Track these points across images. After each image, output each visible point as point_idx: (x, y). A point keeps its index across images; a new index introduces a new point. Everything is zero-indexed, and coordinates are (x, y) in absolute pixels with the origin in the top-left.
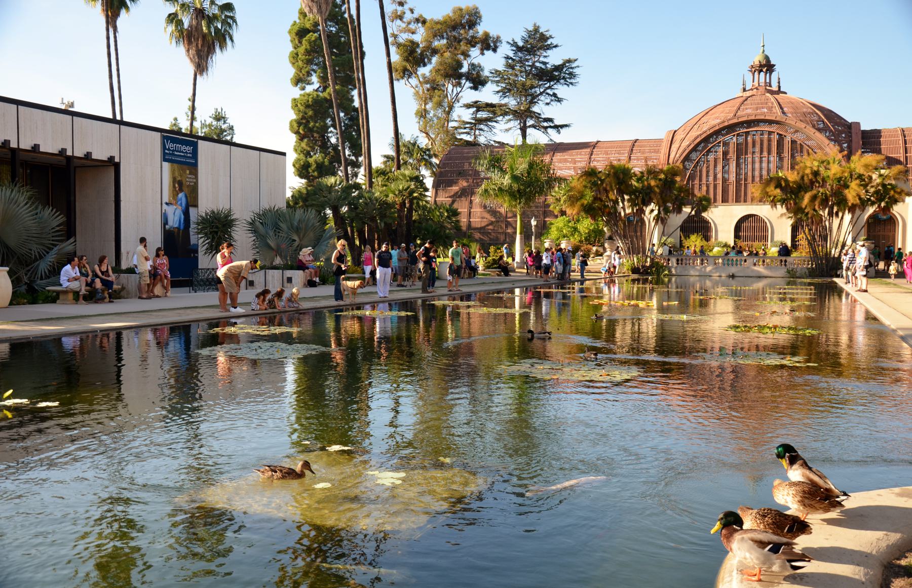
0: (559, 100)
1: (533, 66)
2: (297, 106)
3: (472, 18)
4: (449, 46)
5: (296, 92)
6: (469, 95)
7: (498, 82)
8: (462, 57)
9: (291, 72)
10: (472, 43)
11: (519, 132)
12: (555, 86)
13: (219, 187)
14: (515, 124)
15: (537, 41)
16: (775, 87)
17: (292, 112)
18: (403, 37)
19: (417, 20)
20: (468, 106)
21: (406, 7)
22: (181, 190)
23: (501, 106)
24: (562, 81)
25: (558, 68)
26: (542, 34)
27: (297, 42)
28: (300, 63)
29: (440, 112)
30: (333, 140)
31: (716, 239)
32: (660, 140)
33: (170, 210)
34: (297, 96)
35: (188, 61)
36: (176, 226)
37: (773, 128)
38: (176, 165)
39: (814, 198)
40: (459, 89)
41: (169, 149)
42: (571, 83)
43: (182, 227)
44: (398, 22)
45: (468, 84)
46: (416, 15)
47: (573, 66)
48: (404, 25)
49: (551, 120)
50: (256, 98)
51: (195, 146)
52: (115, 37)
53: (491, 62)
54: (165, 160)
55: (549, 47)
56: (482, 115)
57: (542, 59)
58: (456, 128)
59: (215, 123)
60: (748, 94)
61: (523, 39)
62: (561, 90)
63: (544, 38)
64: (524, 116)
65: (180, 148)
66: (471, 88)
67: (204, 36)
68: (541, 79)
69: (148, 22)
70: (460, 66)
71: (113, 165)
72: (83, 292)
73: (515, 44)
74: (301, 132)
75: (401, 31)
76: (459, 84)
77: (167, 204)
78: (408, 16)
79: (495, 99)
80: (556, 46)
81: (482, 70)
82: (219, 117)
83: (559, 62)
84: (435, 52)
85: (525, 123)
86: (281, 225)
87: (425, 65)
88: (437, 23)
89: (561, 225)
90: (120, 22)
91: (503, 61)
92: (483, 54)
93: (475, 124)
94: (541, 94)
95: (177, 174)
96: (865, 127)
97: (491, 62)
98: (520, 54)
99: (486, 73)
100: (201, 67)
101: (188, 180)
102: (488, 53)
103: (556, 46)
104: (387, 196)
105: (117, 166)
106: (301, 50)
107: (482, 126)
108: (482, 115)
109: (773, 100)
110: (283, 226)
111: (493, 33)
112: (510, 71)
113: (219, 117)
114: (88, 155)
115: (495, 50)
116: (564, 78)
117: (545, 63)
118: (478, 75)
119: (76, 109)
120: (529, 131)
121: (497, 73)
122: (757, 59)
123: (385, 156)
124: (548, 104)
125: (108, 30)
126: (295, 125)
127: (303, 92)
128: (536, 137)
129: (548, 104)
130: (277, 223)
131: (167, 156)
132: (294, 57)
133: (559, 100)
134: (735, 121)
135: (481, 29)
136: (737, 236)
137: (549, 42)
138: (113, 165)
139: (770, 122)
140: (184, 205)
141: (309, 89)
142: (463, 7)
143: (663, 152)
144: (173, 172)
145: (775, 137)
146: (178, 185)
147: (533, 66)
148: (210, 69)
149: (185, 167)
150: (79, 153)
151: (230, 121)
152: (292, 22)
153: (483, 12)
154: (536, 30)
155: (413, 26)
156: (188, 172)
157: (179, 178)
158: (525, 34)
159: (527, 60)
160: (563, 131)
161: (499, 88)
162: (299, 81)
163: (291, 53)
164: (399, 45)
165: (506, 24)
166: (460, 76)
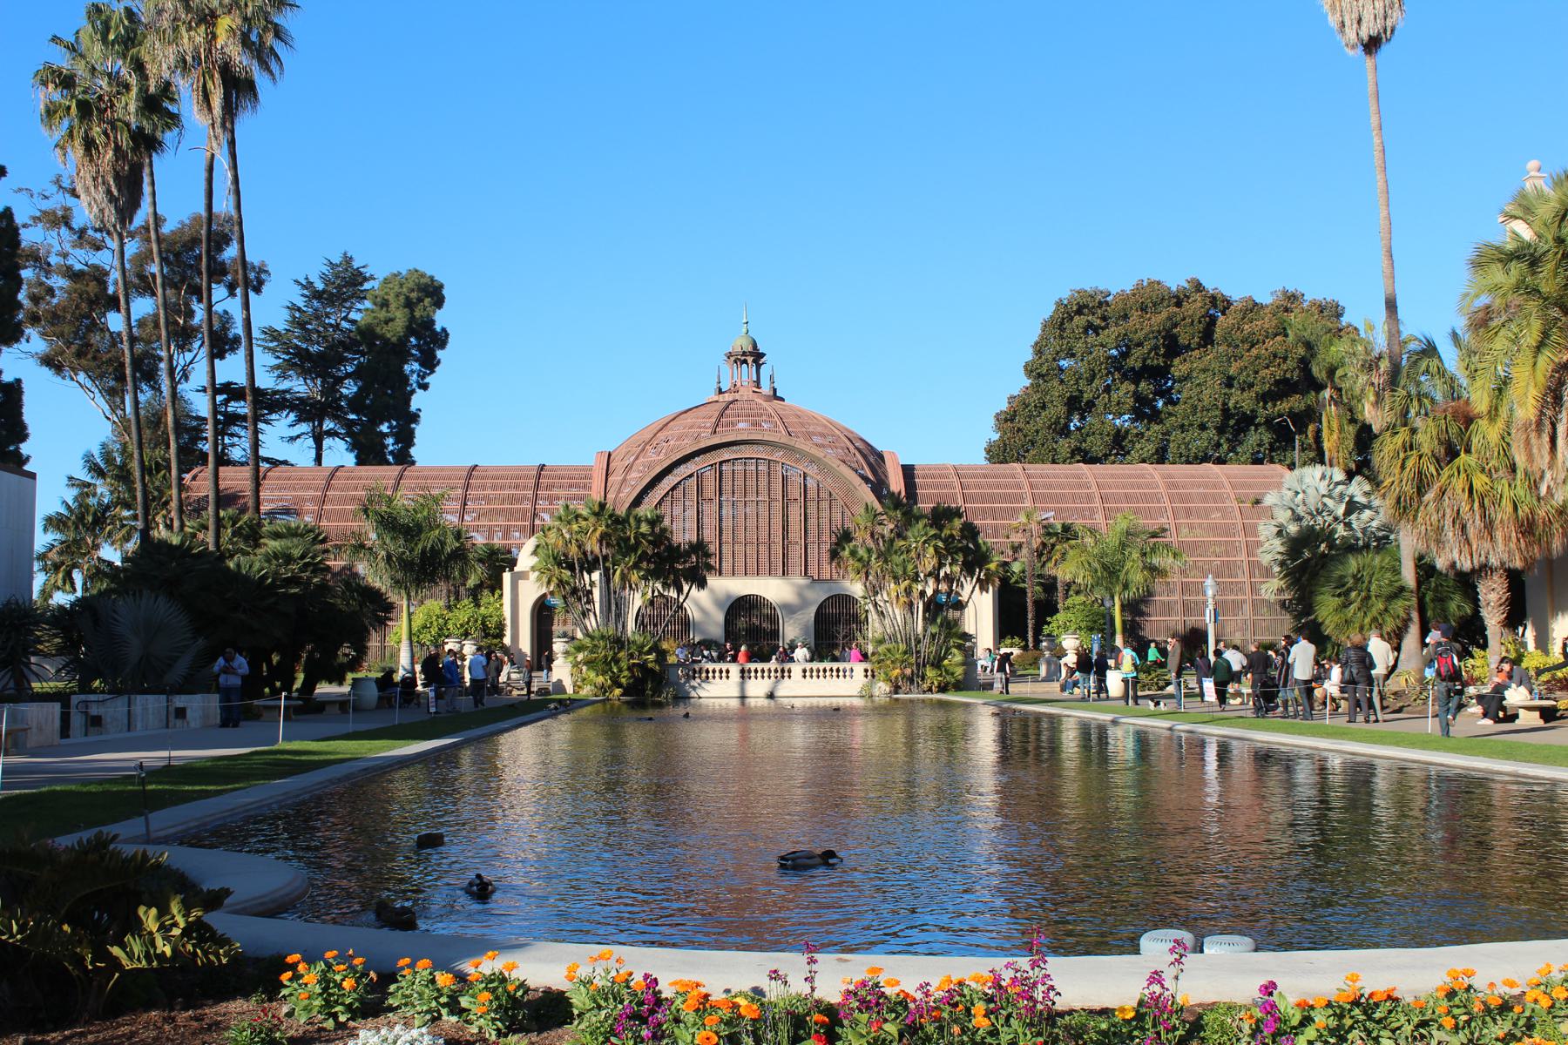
11: (311, 442)
61: (323, 277)
73: (309, 285)
91: (286, 315)
120: (327, 442)
154: (348, 260)
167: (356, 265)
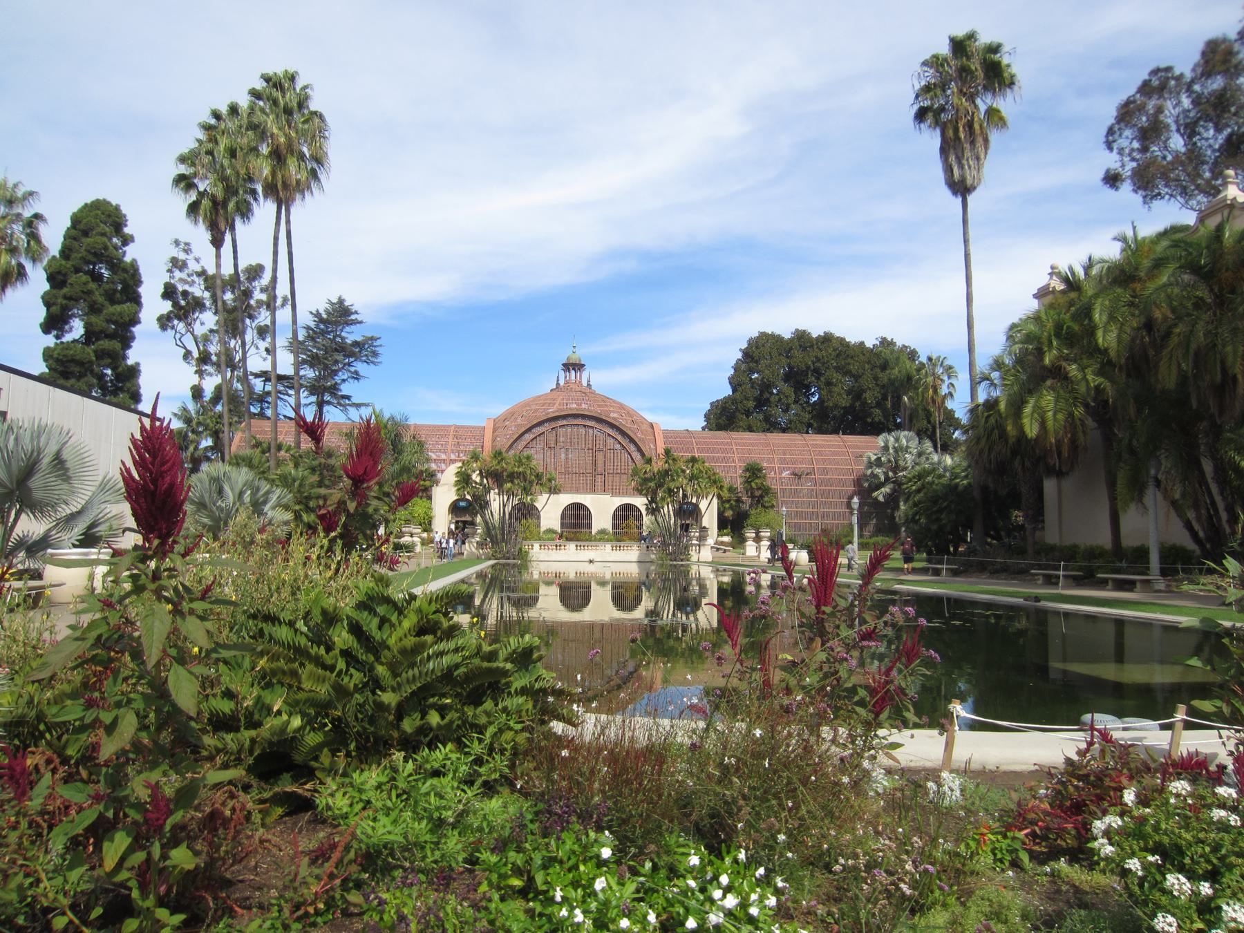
5: (50, 341)
15: (341, 314)
17: (44, 364)
25: (356, 344)
49: (348, 398)
57: (343, 334)
62: (360, 367)
73: (318, 315)
83: (359, 339)
120: (326, 408)
137: (353, 317)
141: (68, 338)
154: (341, 301)
158: (328, 306)
159: (329, 333)
163: (46, 294)
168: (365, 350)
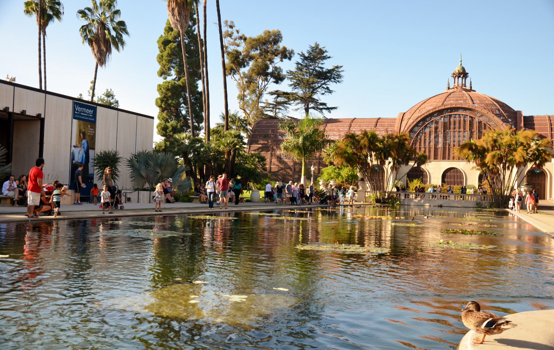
0: (330, 92)
1: (314, 70)
2: (161, 89)
3: (276, 38)
4: (261, 54)
5: (161, 81)
6: (272, 86)
7: (291, 78)
8: (269, 63)
9: (158, 67)
10: (275, 53)
11: (304, 111)
12: (328, 83)
13: (108, 137)
14: (302, 106)
15: (317, 54)
16: (468, 87)
18: (231, 48)
19: (241, 38)
20: (272, 94)
21: (234, 29)
22: (84, 138)
23: (293, 94)
24: (333, 80)
25: (330, 71)
26: (321, 50)
27: (162, 48)
28: (164, 62)
29: (254, 97)
30: (184, 112)
31: (430, 183)
32: (395, 119)
33: (76, 151)
34: (161, 83)
35: (93, 56)
36: (80, 161)
37: (468, 113)
38: (81, 122)
39: (494, 156)
40: (266, 83)
41: (77, 111)
42: (338, 81)
43: (84, 162)
44: (229, 38)
45: (272, 80)
46: (240, 35)
47: (340, 70)
48: (232, 41)
50: (135, 84)
51: (95, 110)
52: (44, 39)
53: (287, 66)
54: (75, 118)
55: (325, 58)
56: (281, 99)
57: (320, 65)
58: (264, 107)
59: (106, 98)
60: (451, 91)
61: (308, 52)
62: (331, 85)
63: (322, 52)
64: (308, 101)
65: (85, 112)
66: (274, 82)
67: (104, 40)
68: (319, 78)
69: (67, 31)
70: (268, 68)
71: (40, 120)
72: (16, 198)
73: (303, 55)
74: (163, 106)
75: (230, 44)
76: (266, 80)
77: (74, 146)
78: (235, 35)
79: (289, 90)
80: (329, 57)
81: (282, 71)
82: (109, 95)
83: (330, 68)
84: (251, 58)
85: (308, 105)
86: (150, 162)
87: (244, 67)
88: (254, 40)
89: (330, 171)
90: (48, 29)
91: (295, 66)
92: (282, 61)
93: (276, 105)
94: (319, 87)
95: (82, 127)
96: (525, 113)
97: (287, 66)
98: (306, 62)
99: (284, 73)
100: (102, 60)
101: (89, 131)
102: (286, 61)
103: (329, 57)
104: (219, 147)
105: (42, 121)
106: (165, 53)
107: (280, 107)
108: (281, 99)
109: (467, 95)
110: (151, 163)
111: (289, 48)
112: (300, 72)
113: (109, 95)
114: (23, 112)
115: (290, 59)
116: (334, 78)
117: (322, 68)
118: (279, 74)
119: (17, 82)
120: (310, 111)
121: (291, 73)
122: (457, 69)
123: (217, 124)
124: (323, 94)
125: (40, 34)
126: (159, 102)
127: (165, 81)
128: (315, 114)
129: (323, 94)
130: (147, 161)
131: (76, 116)
132: (160, 58)
133: (330, 92)
134: (443, 107)
135: (281, 45)
136: (443, 181)
137: (325, 55)
138: (40, 120)
139: (465, 109)
140: (85, 148)
141: (169, 79)
142: (271, 31)
143: (396, 126)
144: (79, 126)
145: (468, 119)
146: (82, 135)
147: (314, 70)
148: (107, 63)
149: (88, 123)
150: (17, 110)
151: (116, 98)
152: (160, 36)
153: (283, 34)
154: (317, 46)
155: (238, 41)
156: (89, 126)
157: (83, 130)
158: (309, 49)
159: (311, 66)
160: (332, 111)
161: (292, 83)
162: (163, 73)
163: (159, 55)
164: (229, 53)
165: (298, 43)
166: (267, 75)
167: (320, 47)
168: (331, 75)
